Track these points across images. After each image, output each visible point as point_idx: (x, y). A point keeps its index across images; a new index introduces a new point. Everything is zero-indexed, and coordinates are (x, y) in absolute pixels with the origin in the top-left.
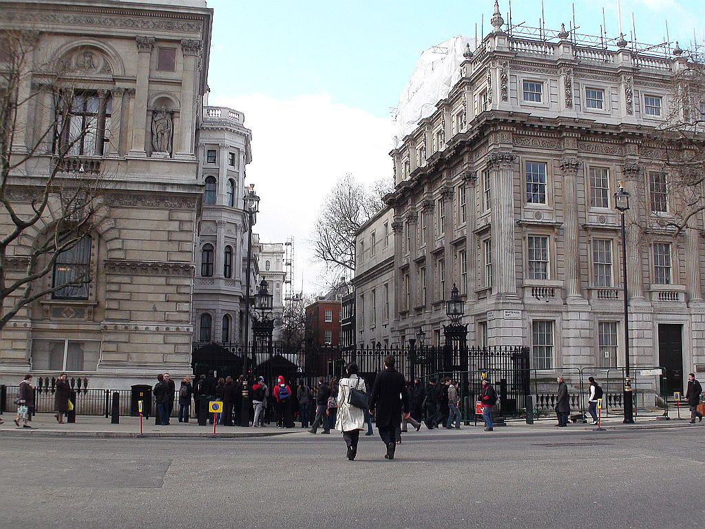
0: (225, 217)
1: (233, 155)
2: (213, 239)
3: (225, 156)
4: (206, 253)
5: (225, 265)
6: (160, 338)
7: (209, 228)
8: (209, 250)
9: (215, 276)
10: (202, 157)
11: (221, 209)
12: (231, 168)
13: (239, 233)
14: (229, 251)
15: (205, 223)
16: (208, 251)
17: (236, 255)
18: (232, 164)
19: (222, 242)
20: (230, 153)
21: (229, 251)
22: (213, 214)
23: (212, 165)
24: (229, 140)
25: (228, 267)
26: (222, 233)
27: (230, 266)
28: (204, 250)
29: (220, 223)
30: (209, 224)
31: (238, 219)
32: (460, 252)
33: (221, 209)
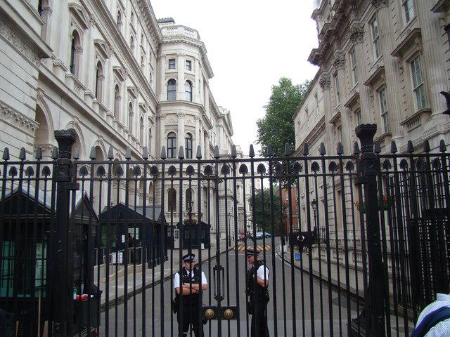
0: (184, 110)
1: (190, 62)
3: (181, 63)
4: (170, 140)
10: (164, 64)
13: (198, 123)
14: (190, 137)
16: (172, 138)
18: (190, 70)
19: (183, 130)
20: (187, 61)
21: (190, 137)
22: (175, 108)
24: (183, 49)
26: (182, 123)
29: (180, 114)
30: (172, 116)
31: (196, 112)
32: (408, 61)
33: (182, 103)
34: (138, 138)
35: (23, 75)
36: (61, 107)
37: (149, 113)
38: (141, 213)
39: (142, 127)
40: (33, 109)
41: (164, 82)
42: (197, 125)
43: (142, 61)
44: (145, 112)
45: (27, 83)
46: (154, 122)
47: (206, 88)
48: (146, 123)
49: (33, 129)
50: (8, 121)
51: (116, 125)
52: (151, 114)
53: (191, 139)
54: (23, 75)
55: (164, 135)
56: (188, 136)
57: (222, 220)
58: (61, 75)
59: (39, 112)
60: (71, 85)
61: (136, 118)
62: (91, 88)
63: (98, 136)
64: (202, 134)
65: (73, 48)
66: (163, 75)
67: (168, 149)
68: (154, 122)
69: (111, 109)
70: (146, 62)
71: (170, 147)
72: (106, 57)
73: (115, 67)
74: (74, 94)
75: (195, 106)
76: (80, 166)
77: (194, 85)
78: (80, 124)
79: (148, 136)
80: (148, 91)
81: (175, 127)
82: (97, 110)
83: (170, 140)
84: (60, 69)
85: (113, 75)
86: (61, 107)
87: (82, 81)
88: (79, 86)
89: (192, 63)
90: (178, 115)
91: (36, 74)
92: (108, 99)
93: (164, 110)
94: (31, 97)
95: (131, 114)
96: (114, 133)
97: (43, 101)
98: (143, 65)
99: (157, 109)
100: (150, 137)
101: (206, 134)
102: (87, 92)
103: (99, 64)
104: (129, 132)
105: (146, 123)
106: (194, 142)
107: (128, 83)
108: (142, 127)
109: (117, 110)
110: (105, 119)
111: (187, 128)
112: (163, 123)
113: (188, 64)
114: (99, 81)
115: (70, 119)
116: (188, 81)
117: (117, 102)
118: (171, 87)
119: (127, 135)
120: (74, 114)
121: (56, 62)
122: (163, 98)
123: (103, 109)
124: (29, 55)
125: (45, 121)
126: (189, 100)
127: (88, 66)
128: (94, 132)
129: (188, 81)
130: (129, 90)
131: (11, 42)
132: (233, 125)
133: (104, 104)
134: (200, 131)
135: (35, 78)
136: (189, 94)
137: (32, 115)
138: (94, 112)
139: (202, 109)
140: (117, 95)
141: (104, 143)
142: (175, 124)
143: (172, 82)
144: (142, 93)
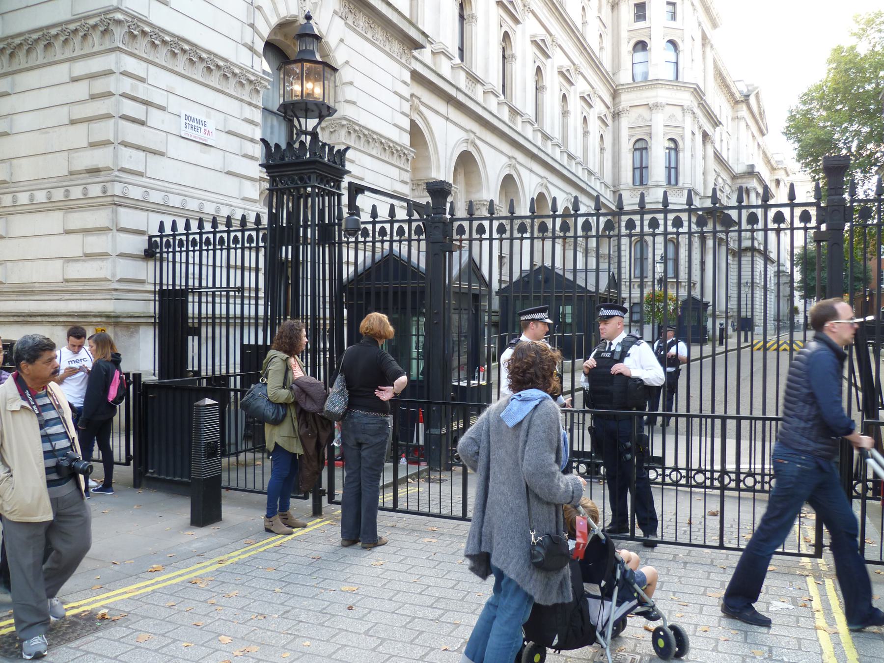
0: (662, 95)
1: (674, 4)
2: (646, 130)
4: (638, 153)
5: (669, 168)
6: (54, 221)
7: (640, 116)
8: (641, 147)
9: (650, 183)
11: (656, 83)
12: (672, 24)
13: (689, 118)
14: (675, 147)
15: (634, 109)
16: (641, 149)
17: (683, 150)
21: (675, 147)
23: (641, 24)
25: (673, 170)
26: (659, 121)
27: (676, 168)
28: (635, 150)
29: (656, 106)
31: (687, 98)
33: (656, 83)
34: (579, 154)
35: (388, 81)
36: (447, 119)
37: (599, 108)
38: (571, 278)
39: (586, 133)
40: (405, 130)
41: (626, 47)
42: (689, 125)
43: (584, 16)
44: (590, 106)
45: (395, 93)
46: (609, 121)
47: (708, 49)
48: (594, 125)
49: (408, 160)
50: (374, 153)
51: (539, 135)
52: (604, 110)
53: (676, 149)
54: (388, 81)
55: (626, 146)
56: (672, 145)
57: (733, 292)
58: (445, 67)
59: (415, 132)
60: (462, 80)
61: (575, 120)
62: (495, 80)
63: (510, 157)
64: (699, 137)
65: (462, 17)
66: (624, 35)
67: (634, 169)
68: (609, 121)
69: (529, 110)
70: (592, 14)
71: (638, 165)
72: (517, 21)
73: (535, 36)
74: (466, 95)
75: (684, 86)
76: (456, 224)
77: (681, 46)
78: (478, 142)
79: (598, 150)
80: (597, 66)
81: (646, 130)
82: (505, 114)
83: (638, 153)
84: (443, 57)
85: (532, 50)
86: (447, 119)
87: (479, 72)
88: (474, 79)
89: (678, 7)
90: (652, 107)
91: (407, 76)
92: (523, 96)
93: (626, 100)
94: (403, 113)
95: (565, 113)
96: (535, 151)
97: (420, 113)
98: (584, 23)
99: (614, 98)
100: (602, 149)
101: (705, 136)
102: (488, 87)
103: (506, 36)
104: (563, 146)
105: (594, 125)
106: (681, 155)
107: (558, 60)
108: (586, 133)
109: (539, 108)
110: (519, 129)
111: (668, 129)
112: (625, 122)
113: (670, 8)
114: (508, 66)
115: (463, 135)
116: (672, 42)
117: (539, 95)
118: (640, 56)
119: (558, 150)
120: (468, 128)
121: (436, 47)
122: (624, 77)
123: (514, 112)
124: (396, 47)
125: (426, 144)
126: (672, 77)
127: (487, 43)
128: (502, 152)
129: (672, 42)
130: (561, 73)
131: (369, 36)
132: (767, 115)
133: (518, 104)
134: (693, 134)
135: (405, 83)
136: (672, 66)
137: (406, 140)
138: (500, 119)
139: (698, 93)
140: (540, 84)
141: (518, 166)
142: (648, 124)
143: (641, 46)
144: (583, 71)
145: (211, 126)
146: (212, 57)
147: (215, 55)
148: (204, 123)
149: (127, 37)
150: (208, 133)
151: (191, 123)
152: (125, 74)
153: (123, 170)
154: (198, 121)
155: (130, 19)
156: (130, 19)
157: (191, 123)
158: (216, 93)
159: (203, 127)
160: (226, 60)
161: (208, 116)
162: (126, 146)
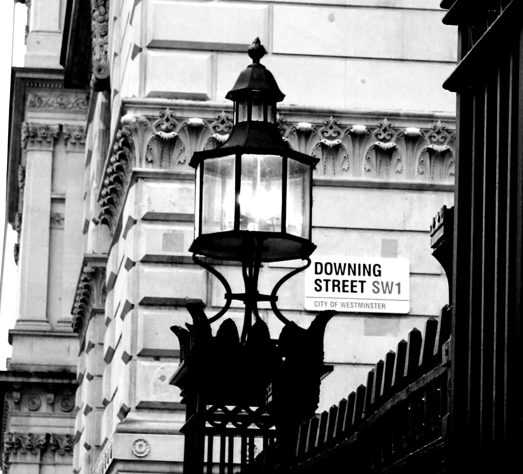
145: (395, 270)
146: (386, 122)
147: (394, 116)
148: (373, 270)
149: (156, 149)
150: (388, 288)
151: (333, 276)
152: (151, 218)
153: (143, 407)
154: (352, 269)
155: (157, 114)
156: (157, 114)
157: (333, 276)
158: (414, 196)
159: (370, 280)
160: (431, 118)
161: (390, 251)
162: (157, 358)
